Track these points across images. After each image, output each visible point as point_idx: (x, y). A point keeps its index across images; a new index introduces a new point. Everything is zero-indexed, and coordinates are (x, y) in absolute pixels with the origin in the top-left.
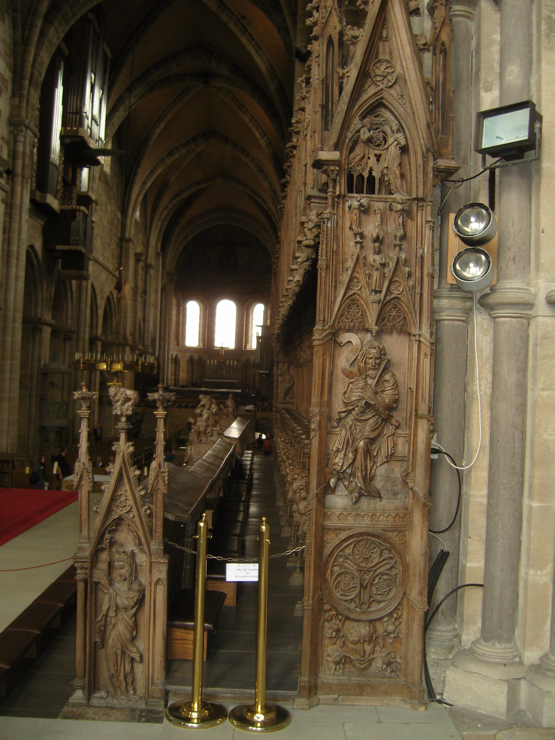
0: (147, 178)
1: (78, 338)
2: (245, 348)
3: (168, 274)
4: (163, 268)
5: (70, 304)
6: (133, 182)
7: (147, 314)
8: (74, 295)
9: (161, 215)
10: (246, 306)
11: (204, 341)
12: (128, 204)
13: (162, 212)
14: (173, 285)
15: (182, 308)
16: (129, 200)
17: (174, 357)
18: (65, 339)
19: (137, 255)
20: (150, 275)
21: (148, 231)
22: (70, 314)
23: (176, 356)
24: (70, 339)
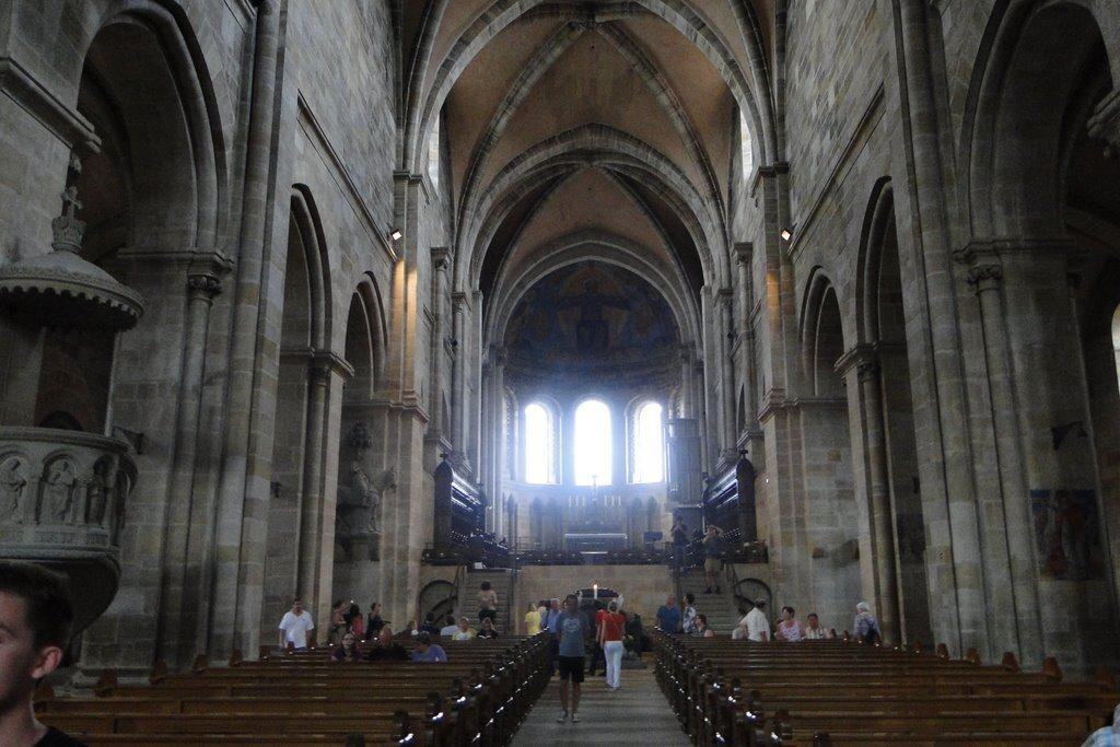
0: (451, 54)
1: (239, 288)
2: (631, 481)
3: (492, 346)
4: (485, 338)
5: (213, 176)
6: (421, 55)
7: (458, 389)
8: (229, 152)
9: (480, 203)
10: (627, 408)
11: (556, 472)
12: (412, 104)
13: (482, 199)
14: (502, 368)
15: (517, 414)
16: (414, 95)
17: (507, 499)
18: (191, 290)
19: (434, 252)
20: (463, 316)
21: (456, 230)
22: (211, 209)
23: (511, 496)
24: (213, 292)
